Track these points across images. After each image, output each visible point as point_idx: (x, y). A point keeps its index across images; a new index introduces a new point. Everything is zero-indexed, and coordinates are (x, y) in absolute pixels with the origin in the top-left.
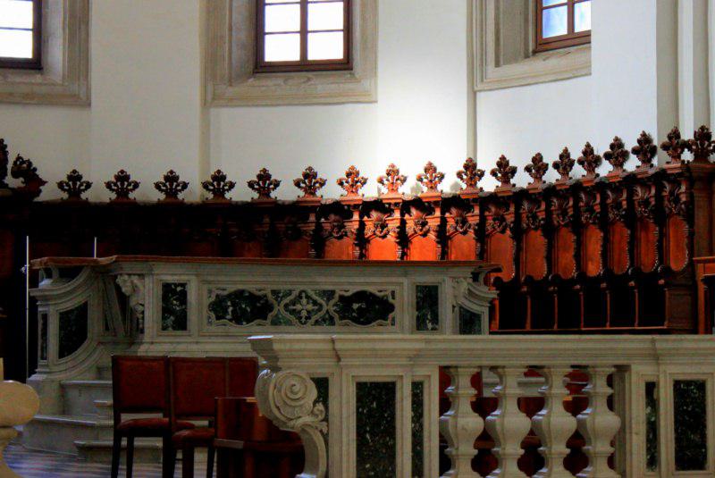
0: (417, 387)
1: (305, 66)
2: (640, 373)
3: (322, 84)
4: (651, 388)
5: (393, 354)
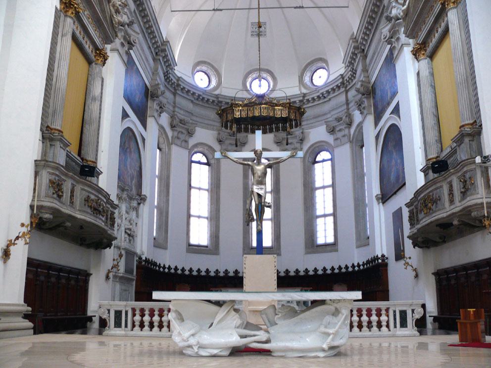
0: (126, 312)
1: (326, 245)
5: (121, 305)
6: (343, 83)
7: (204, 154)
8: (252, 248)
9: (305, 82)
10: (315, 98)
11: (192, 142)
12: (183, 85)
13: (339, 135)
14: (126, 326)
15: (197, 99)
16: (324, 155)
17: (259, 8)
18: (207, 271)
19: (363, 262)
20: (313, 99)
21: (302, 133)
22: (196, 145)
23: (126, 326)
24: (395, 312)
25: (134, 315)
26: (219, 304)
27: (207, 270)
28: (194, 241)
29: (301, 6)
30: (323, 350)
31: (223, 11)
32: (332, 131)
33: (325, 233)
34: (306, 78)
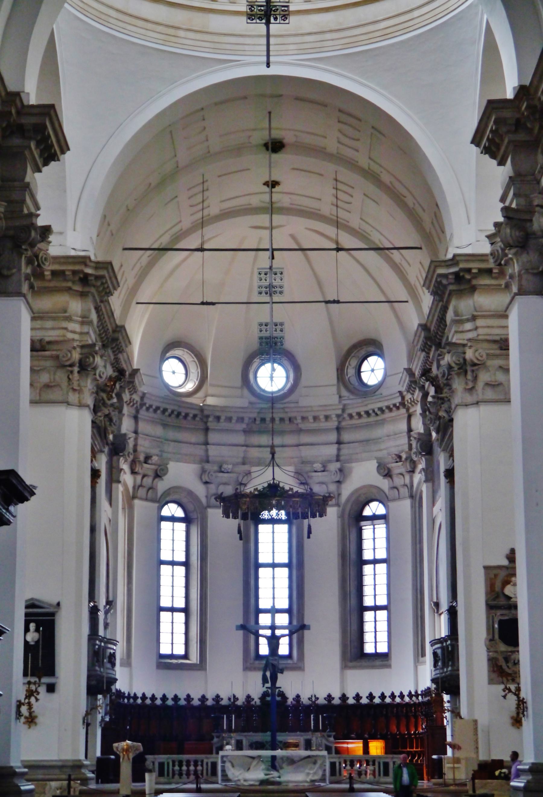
1: (377, 656)
2: (205, 761)
3: (378, 662)
4: (207, 764)
6: (403, 404)
7: (180, 504)
8: (258, 657)
9: (347, 378)
10: (363, 413)
11: (162, 486)
12: (148, 402)
14: (168, 775)
15: (170, 415)
18: (189, 698)
19: (422, 691)
20: (359, 415)
21: (341, 470)
22: (167, 493)
23: (168, 775)
24: (379, 763)
25: (174, 765)
26: (253, 758)
27: (188, 696)
28: (165, 649)
29: (336, 299)
30: (307, 782)
31: (217, 305)
34: (349, 371)
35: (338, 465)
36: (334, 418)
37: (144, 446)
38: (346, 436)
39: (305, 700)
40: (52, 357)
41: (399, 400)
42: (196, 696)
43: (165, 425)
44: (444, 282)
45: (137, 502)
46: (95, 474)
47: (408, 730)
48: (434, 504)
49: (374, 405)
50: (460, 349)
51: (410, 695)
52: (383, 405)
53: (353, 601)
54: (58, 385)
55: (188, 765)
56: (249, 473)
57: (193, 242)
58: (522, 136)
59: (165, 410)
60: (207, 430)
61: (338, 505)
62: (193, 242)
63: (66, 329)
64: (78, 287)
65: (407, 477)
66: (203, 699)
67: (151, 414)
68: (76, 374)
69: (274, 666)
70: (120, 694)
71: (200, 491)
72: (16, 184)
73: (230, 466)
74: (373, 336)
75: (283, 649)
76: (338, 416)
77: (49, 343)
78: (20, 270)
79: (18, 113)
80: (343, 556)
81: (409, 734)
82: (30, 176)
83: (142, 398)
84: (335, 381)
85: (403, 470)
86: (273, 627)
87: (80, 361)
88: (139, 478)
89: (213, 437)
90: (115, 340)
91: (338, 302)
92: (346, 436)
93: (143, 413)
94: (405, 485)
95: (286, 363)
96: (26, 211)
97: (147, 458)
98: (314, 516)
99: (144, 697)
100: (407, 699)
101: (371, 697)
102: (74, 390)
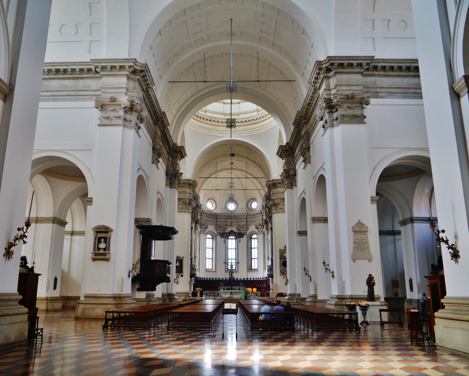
1: (255, 269)
3: (255, 271)
6: (261, 213)
7: (211, 235)
8: (228, 269)
11: (207, 231)
13: (260, 230)
16: (254, 236)
17: (232, 178)
18: (213, 278)
20: (251, 215)
21: (247, 227)
26: (227, 292)
27: (212, 278)
28: (207, 268)
32: (258, 228)
33: (255, 265)
35: (246, 226)
36: (246, 216)
37: (203, 221)
38: (248, 220)
39: (239, 279)
40: (182, 202)
41: (260, 212)
42: (214, 278)
43: (208, 217)
44: (270, 185)
45: (201, 234)
46: (192, 228)
47: (262, 286)
48: (268, 235)
49: (254, 213)
50: (274, 200)
51: (262, 278)
52: (257, 213)
53: (250, 257)
54: (184, 208)
55: (212, 293)
56: (226, 228)
57: (214, 176)
58: (287, 153)
59: (208, 214)
60: (217, 218)
61: (246, 235)
62: (214, 176)
63: (186, 195)
64: (188, 186)
65: (262, 229)
66: (216, 279)
67: (204, 214)
68: (188, 206)
69: (232, 272)
70: (197, 277)
71: (215, 232)
72: (175, 163)
73: (222, 226)
74: (254, 197)
75: (234, 268)
76: (246, 215)
77: (182, 198)
78: (175, 182)
79: (176, 148)
80: (247, 247)
81: (262, 287)
82: (178, 162)
83: (202, 211)
84: (246, 207)
85: (261, 227)
86: (232, 263)
87: (189, 203)
88: (202, 229)
89: (218, 220)
90: (196, 198)
91: (247, 190)
92: (248, 220)
93: (203, 214)
94: (261, 231)
95: (235, 203)
96: (177, 169)
97: (203, 225)
98: (241, 238)
99: (203, 278)
100: (262, 279)
101: (254, 278)
102: (187, 209)
